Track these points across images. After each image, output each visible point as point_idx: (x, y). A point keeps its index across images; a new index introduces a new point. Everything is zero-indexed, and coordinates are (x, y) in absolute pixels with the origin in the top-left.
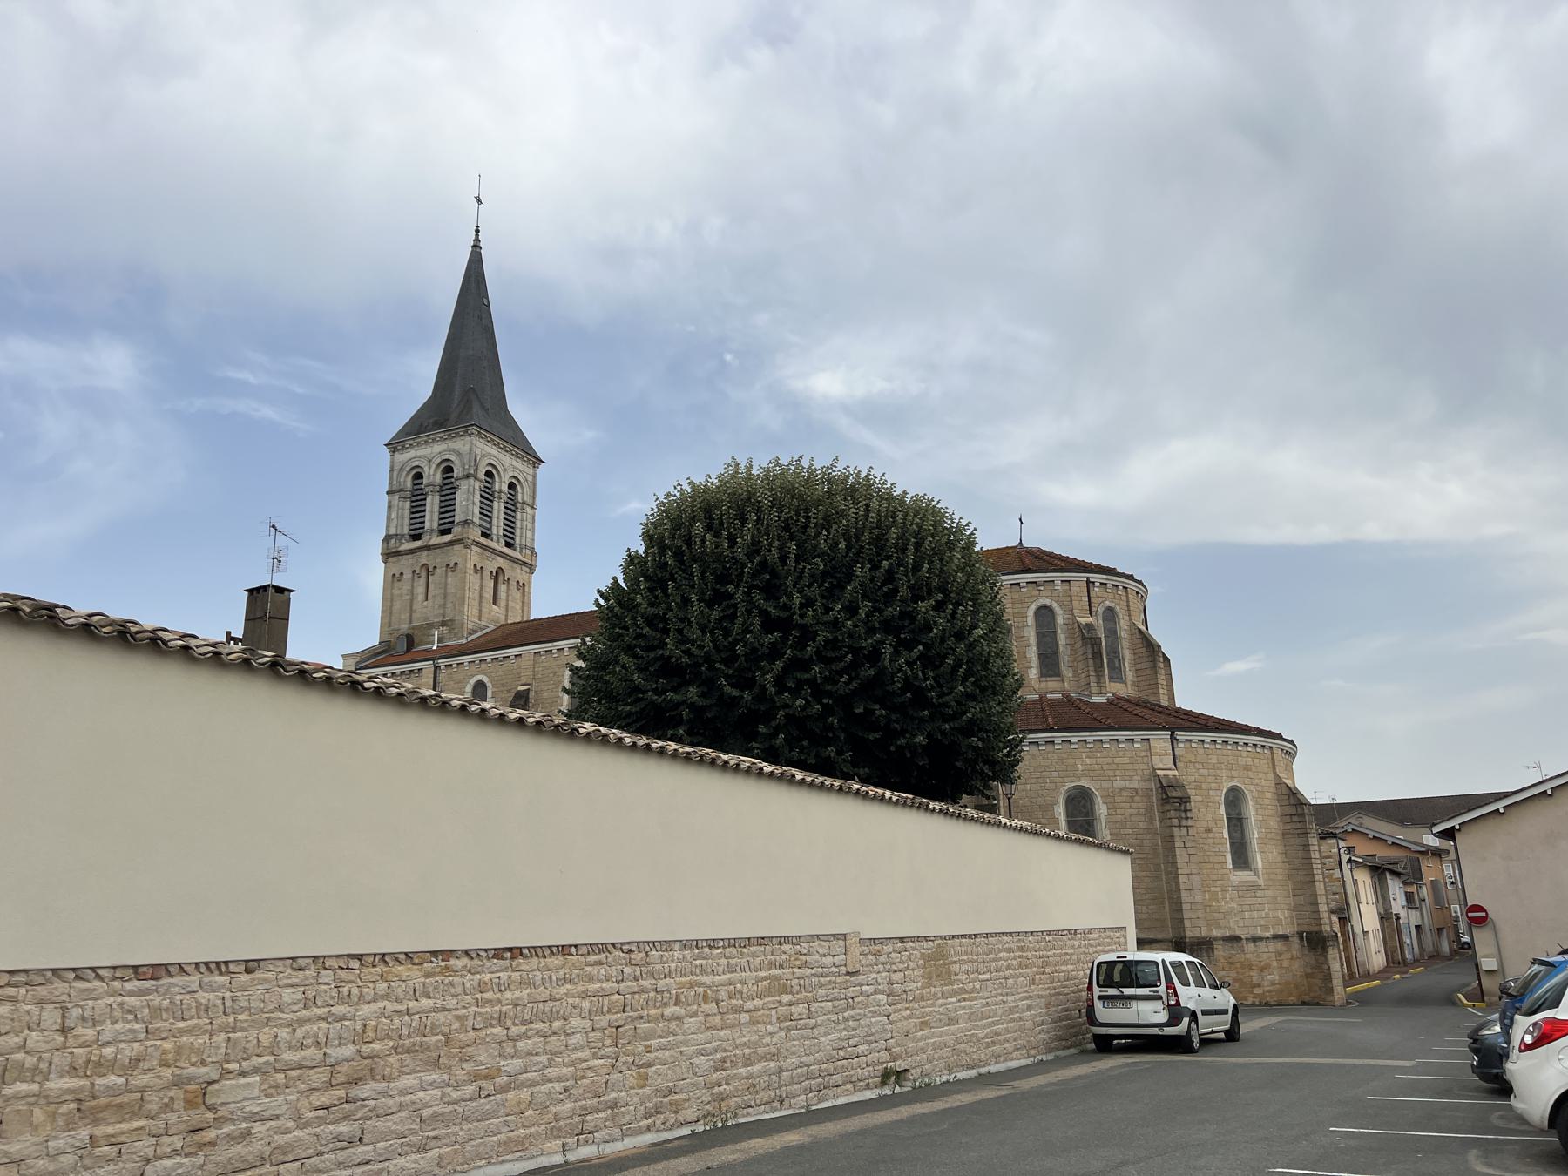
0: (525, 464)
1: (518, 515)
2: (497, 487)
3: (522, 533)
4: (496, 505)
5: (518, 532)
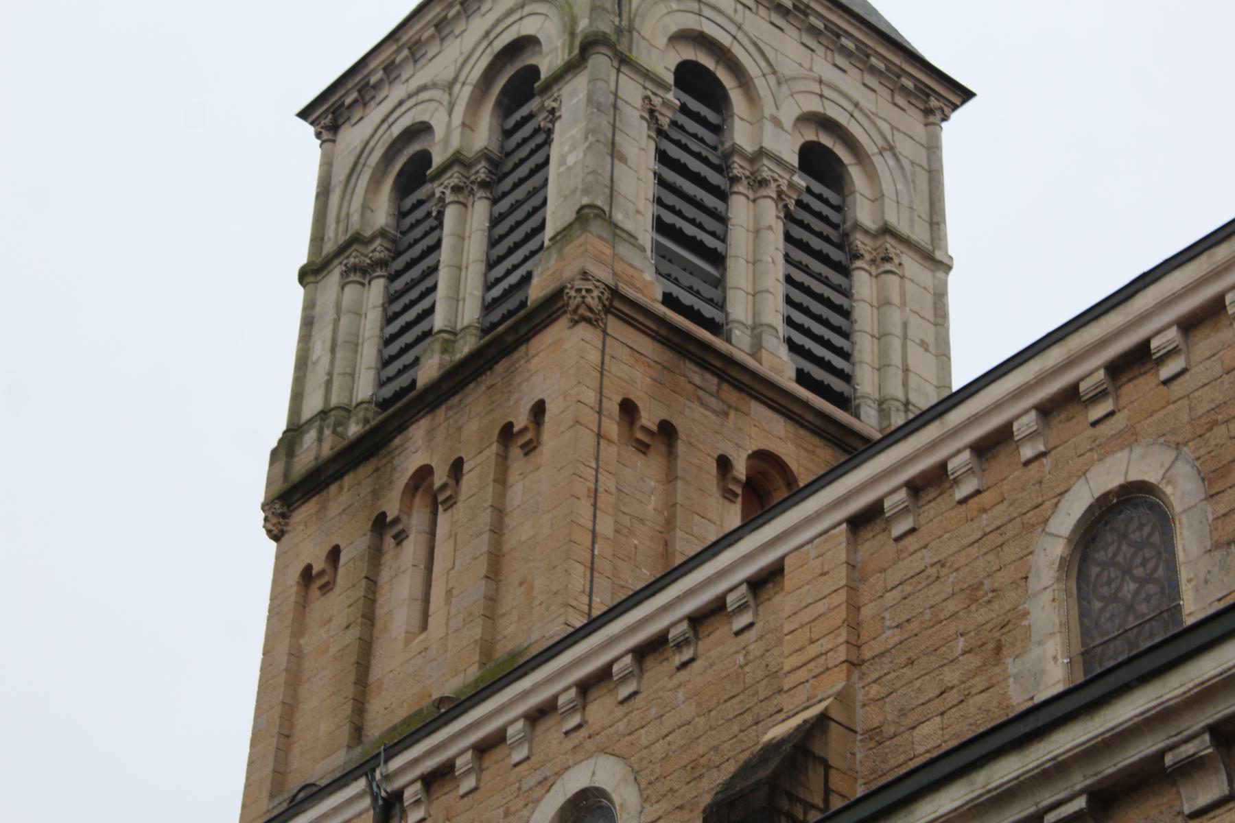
0: (884, 92)
1: (863, 283)
2: (742, 135)
3: (883, 354)
4: (740, 209)
5: (865, 348)
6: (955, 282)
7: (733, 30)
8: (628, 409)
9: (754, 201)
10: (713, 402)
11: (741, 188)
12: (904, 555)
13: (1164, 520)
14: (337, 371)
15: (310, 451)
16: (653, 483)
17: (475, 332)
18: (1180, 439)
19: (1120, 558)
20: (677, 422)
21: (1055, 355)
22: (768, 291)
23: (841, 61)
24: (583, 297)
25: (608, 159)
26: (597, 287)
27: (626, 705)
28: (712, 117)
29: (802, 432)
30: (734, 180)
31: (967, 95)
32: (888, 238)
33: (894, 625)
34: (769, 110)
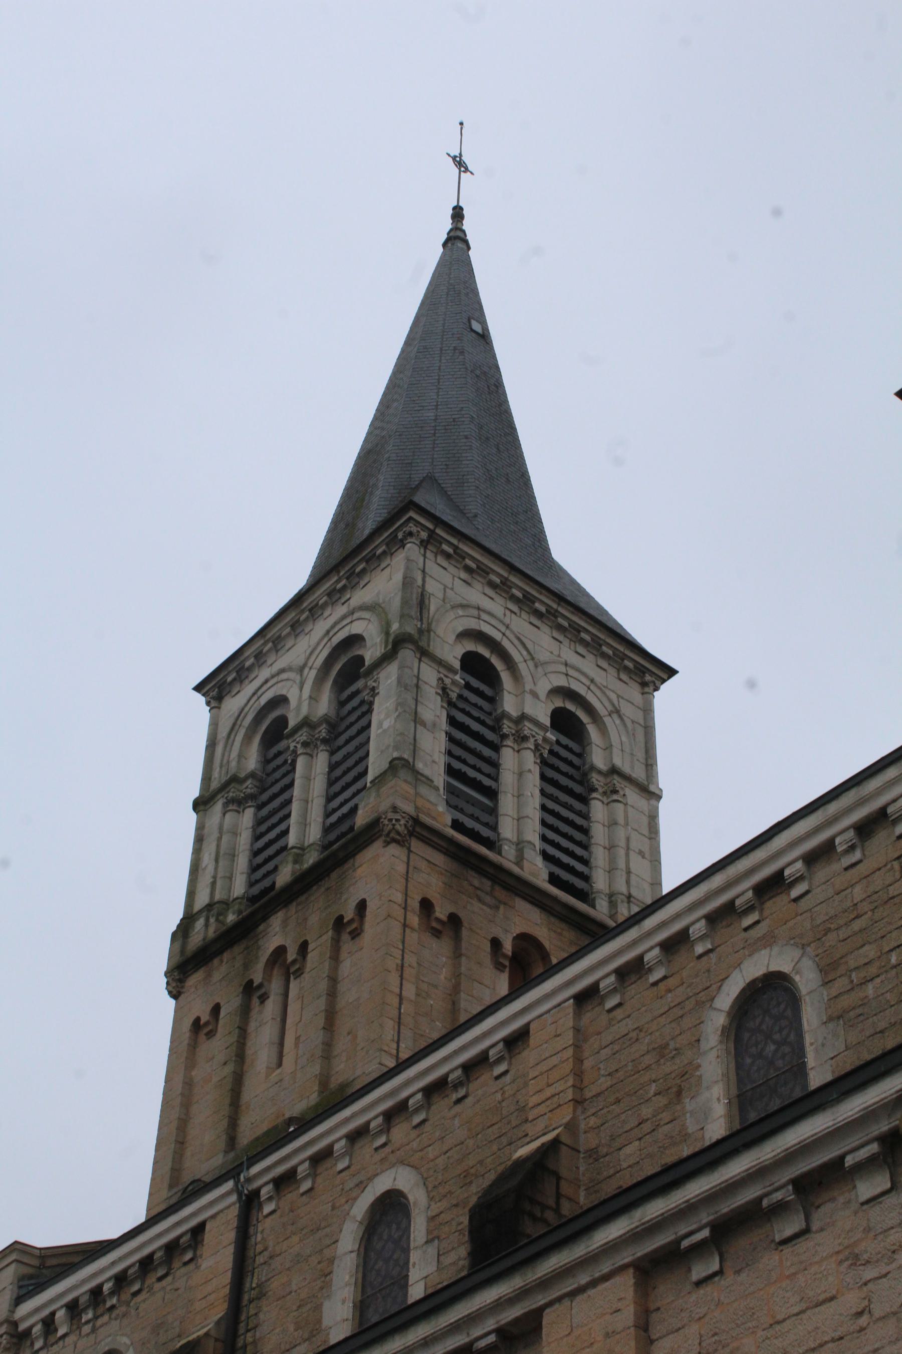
0: (612, 671)
1: (598, 809)
2: (509, 704)
3: (612, 860)
4: (508, 758)
5: (599, 857)
6: (664, 807)
7: (503, 629)
8: (426, 905)
9: (518, 751)
10: (488, 899)
11: (509, 742)
12: (613, 1023)
13: (794, 1000)
14: (220, 875)
15: (199, 933)
16: (444, 959)
17: (317, 848)
18: (804, 941)
19: (764, 1027)
20: (462, 914)
21: (718, 880)
22: (527, 817)
23: (581, 649)
24: (394, 825)
25: (412, 724)
26: (403, 817)
27: (418, 1129)
28: (488, 691)
29: (553, 919)
30: (504, 737)
31: (672, 672)
32: (615, 777)
33: (607, 1073)
34: (528, 686)
